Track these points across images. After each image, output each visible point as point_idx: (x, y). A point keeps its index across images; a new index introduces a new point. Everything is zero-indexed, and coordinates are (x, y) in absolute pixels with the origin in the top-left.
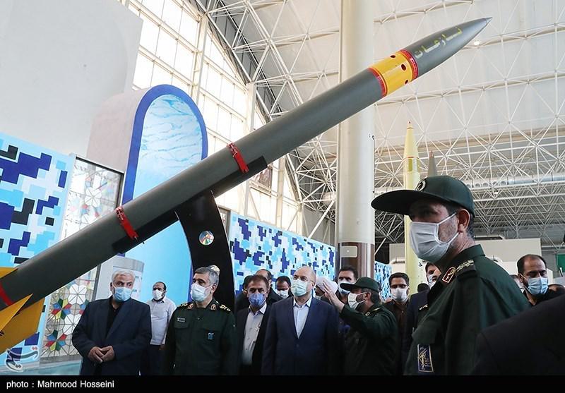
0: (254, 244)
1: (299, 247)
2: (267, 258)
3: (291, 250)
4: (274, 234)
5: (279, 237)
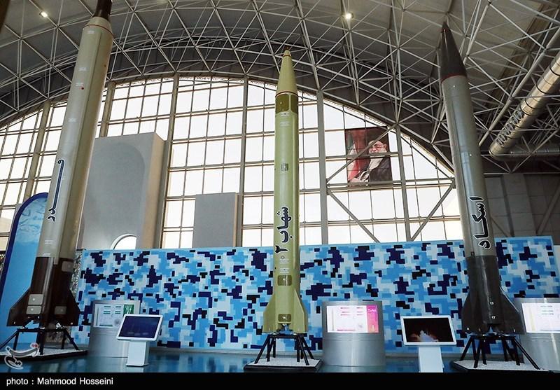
0: (109, 268)
1: (178, 261)
2: (127, 277)
3: (163, 265)
4: (136, 256)
5: (145, 257)
